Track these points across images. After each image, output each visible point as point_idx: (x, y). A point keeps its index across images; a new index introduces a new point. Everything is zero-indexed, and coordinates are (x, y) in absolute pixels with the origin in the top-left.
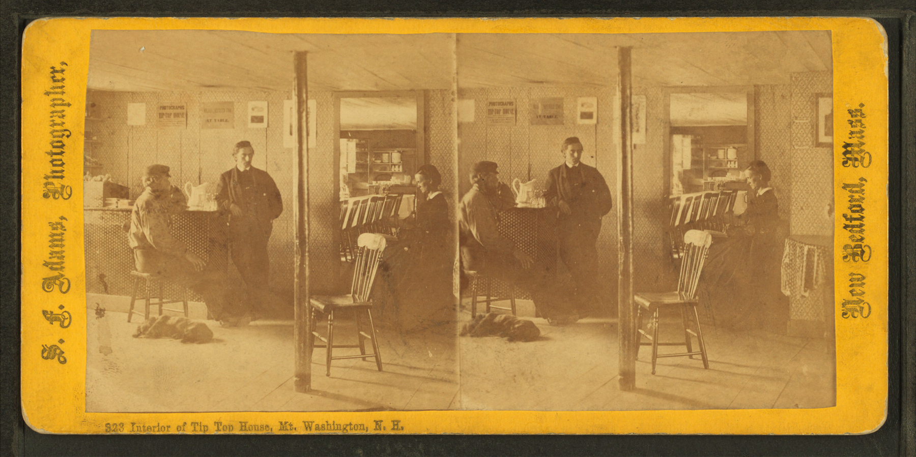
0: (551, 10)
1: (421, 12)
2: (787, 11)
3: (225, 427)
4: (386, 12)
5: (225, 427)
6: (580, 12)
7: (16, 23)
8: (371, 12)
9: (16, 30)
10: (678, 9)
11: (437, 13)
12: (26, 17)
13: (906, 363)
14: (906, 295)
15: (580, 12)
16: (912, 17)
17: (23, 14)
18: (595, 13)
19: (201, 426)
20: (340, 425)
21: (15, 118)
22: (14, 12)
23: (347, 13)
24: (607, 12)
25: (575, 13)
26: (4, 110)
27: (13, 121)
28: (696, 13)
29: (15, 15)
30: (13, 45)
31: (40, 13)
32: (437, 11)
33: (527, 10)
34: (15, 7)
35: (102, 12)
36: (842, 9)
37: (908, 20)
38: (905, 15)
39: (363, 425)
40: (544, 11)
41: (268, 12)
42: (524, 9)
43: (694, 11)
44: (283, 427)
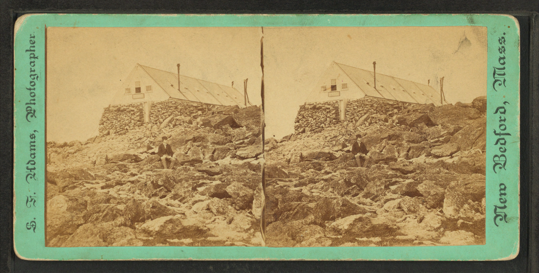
0: (324, 10)
2: (463, 11)
6: (342, 11)
7: (12, 15)
8: (220, 10)
9: (12, 19)
10: (400, 10)
11: (258, 11)
12: (17, 12)
13: (531, 218)
14: (532, 179)
15: (342, 11)
16: (536, 16)
17: (15, 10)
18: (351, 12)
21: (10, 71)
22: (10, 9)
23: (205, 11)
25: (339, 12)
27: (9, 72)
29: (11, 10)
30: (10, 28)
31: (25, 10)
33: (311, 10)
34: (11, 6)
35: (62, 9)
36: (495, 10)
37: (534, 17)
38: (532, 14)
40: (321, 10)
42: (309, 9)
43: (408, 11)
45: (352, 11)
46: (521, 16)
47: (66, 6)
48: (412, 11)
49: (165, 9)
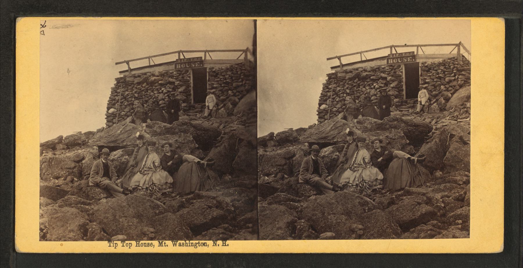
1: (246, 14)
3: (127, 244)
4: (226, 14)
5: (127, 244)
6: (336, 14)
18: (346, 15)
19: (113, 244)
20: (193, 243)
22: (11, 13)
24: (352, 14)
26: (6, 69)
27: (11, 75)
28: (403, 15)
32: (254, 13)
33: (306, 13)
39: (206, 243)
40: (316, 13)
41: (157, 14)
43: (402, 14)
44: (161, 245)
45: (347, 14)
46: (512, 19)
47: (66, 10)
48: (406, 14)
49: (162, 13)
